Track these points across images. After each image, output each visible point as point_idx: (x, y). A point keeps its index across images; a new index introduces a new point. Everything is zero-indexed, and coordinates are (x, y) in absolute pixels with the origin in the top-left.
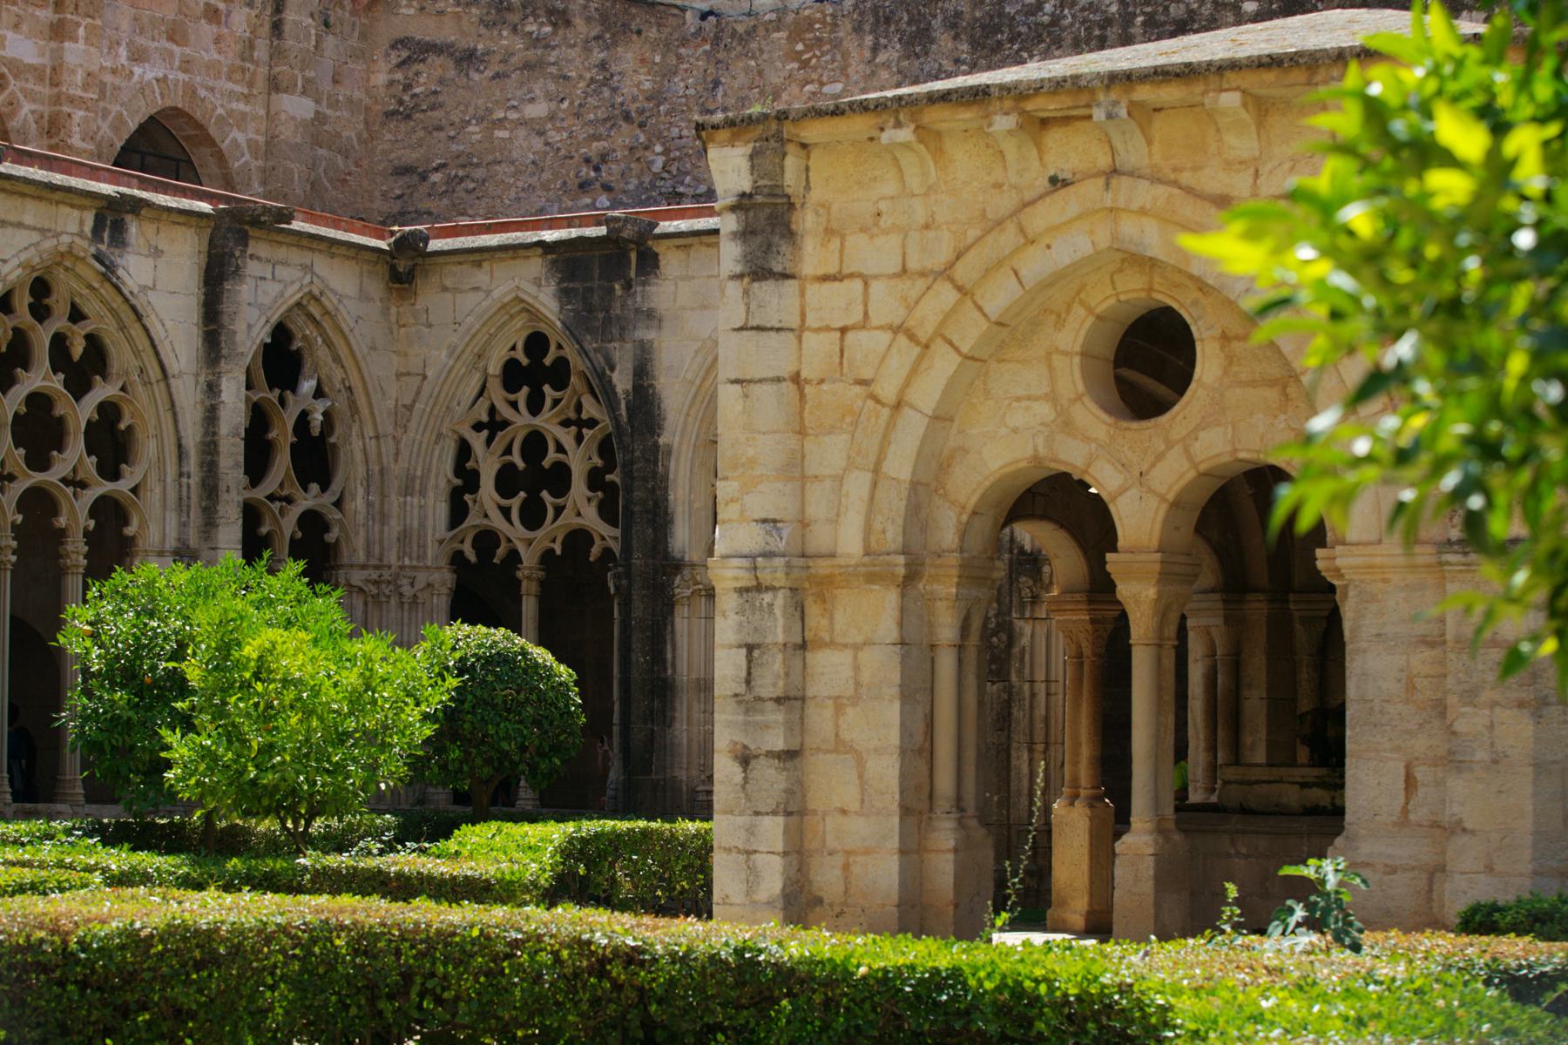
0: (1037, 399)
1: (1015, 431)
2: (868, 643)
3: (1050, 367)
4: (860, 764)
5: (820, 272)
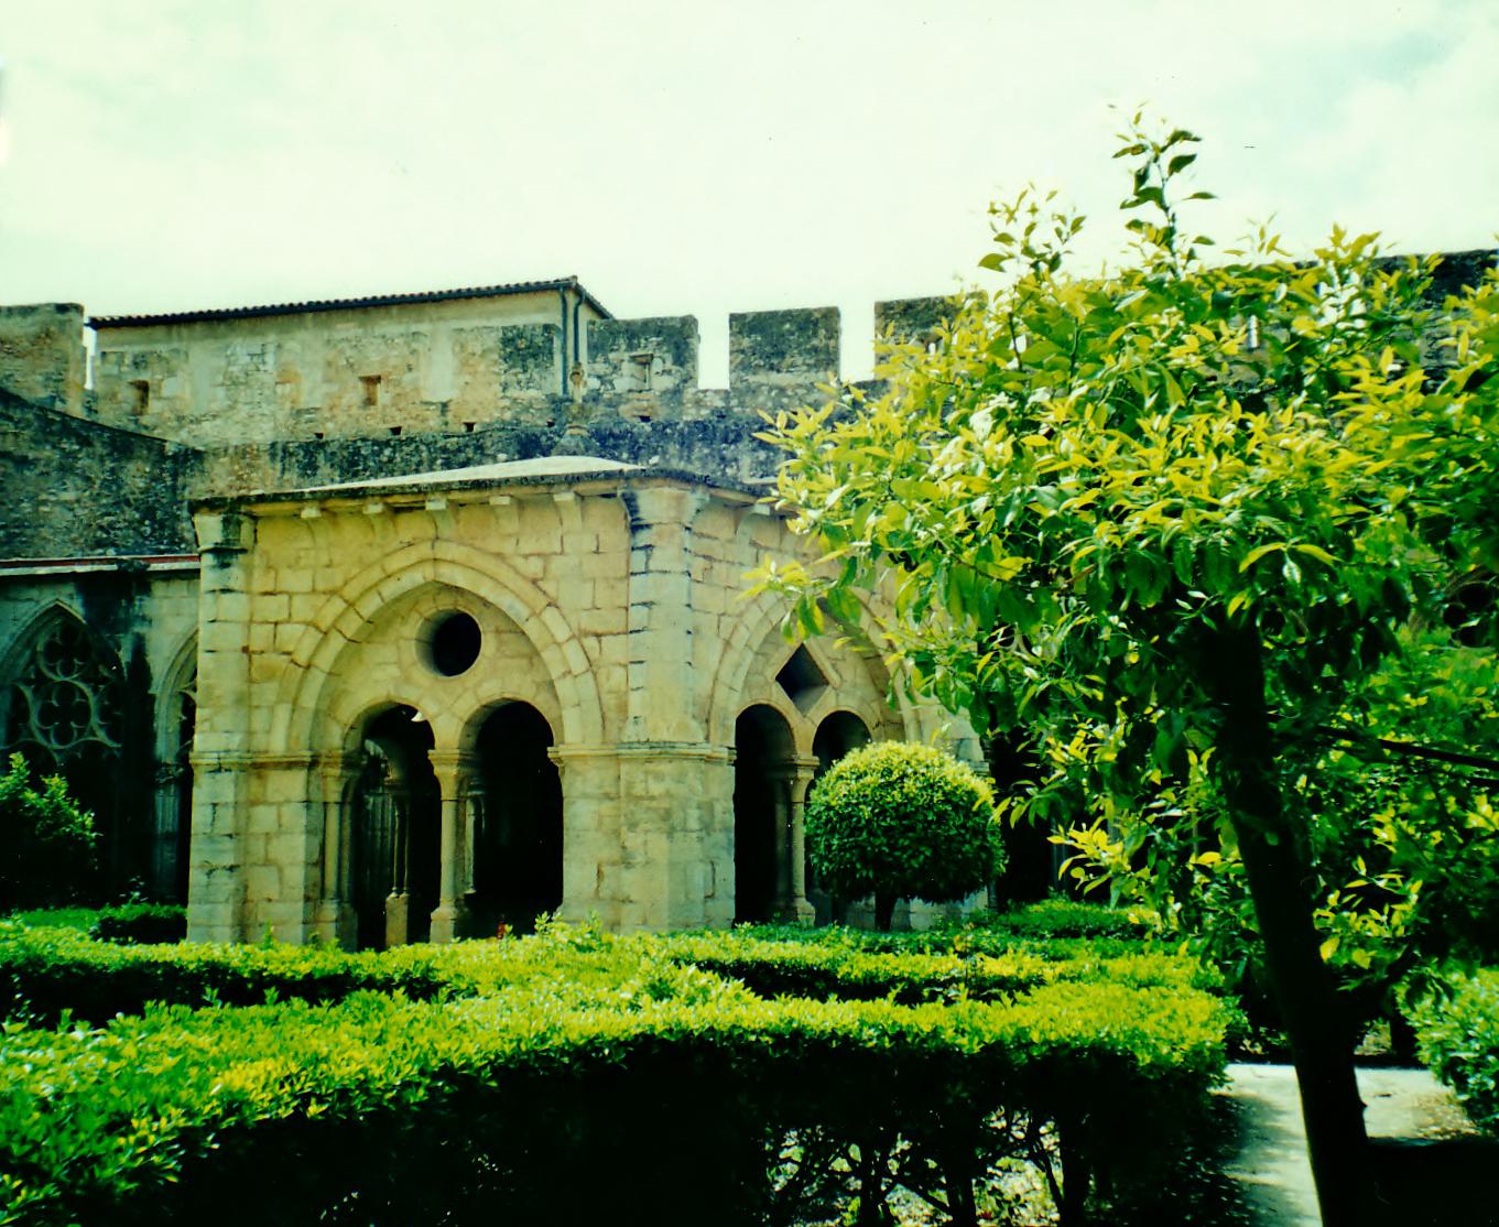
2: (288, 801)
4: (280, 870)
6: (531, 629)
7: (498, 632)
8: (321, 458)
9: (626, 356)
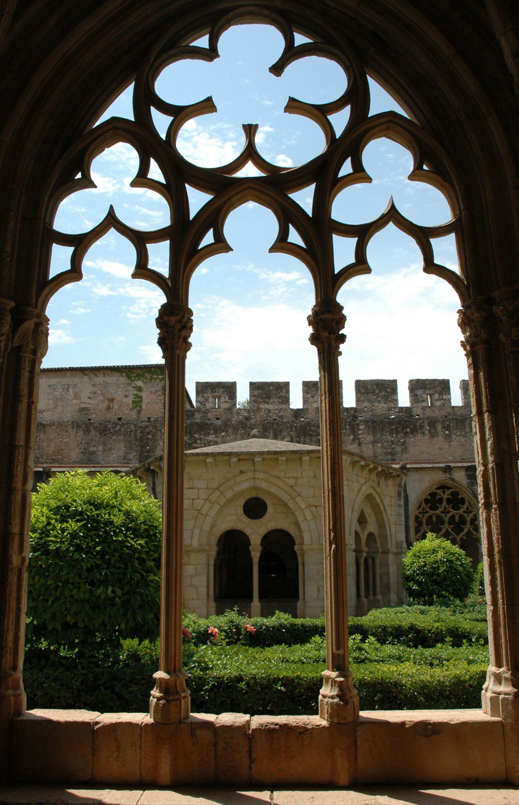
1: (228, 521)
6: (291, 504)
7: (274, 504)
8: (92, 428)
9: (211, 395)
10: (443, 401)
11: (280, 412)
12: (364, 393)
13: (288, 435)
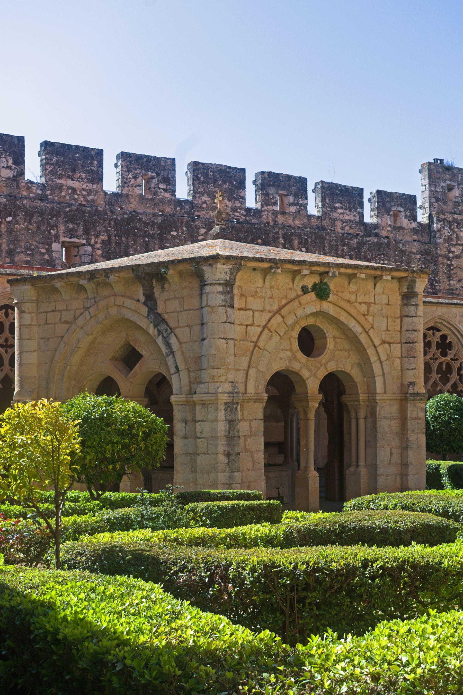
0: (287, 350)
1: (281, 359)
3: (290, 342)
5: (240, 307)
6: (363, 338)
7: (335, 338)
10: (298, 207)
11: (89, 194)
12: (203, 182)
13: (104, 231)
